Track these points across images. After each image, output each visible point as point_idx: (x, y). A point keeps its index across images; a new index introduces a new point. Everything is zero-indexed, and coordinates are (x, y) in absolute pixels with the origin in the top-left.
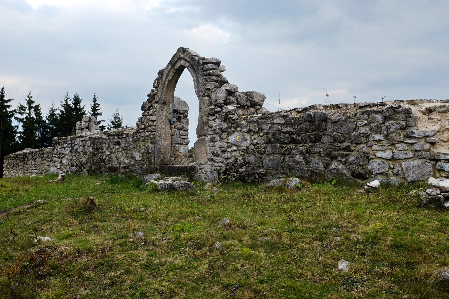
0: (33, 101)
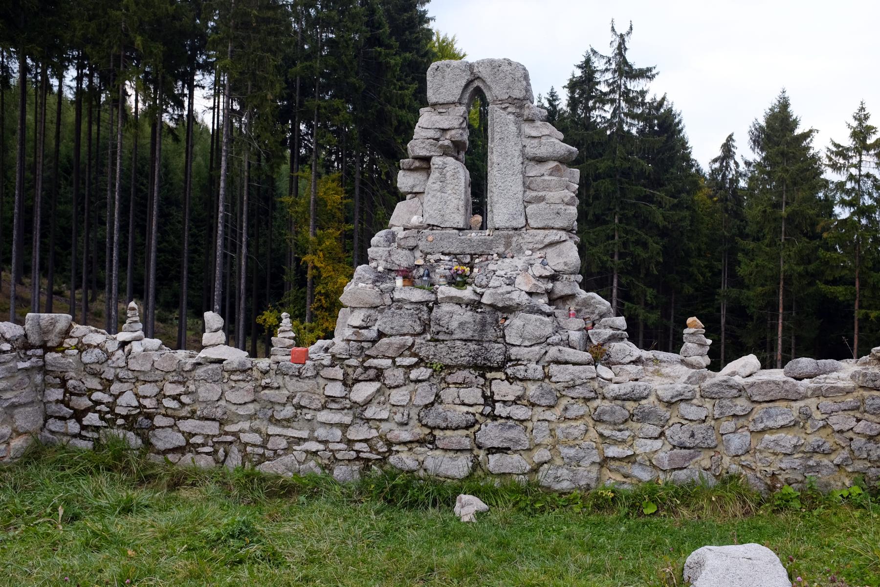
0: (873, 128)
